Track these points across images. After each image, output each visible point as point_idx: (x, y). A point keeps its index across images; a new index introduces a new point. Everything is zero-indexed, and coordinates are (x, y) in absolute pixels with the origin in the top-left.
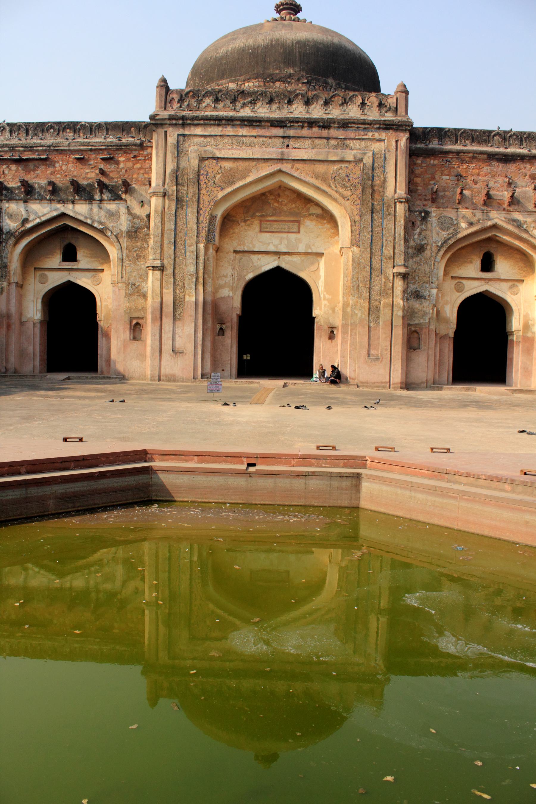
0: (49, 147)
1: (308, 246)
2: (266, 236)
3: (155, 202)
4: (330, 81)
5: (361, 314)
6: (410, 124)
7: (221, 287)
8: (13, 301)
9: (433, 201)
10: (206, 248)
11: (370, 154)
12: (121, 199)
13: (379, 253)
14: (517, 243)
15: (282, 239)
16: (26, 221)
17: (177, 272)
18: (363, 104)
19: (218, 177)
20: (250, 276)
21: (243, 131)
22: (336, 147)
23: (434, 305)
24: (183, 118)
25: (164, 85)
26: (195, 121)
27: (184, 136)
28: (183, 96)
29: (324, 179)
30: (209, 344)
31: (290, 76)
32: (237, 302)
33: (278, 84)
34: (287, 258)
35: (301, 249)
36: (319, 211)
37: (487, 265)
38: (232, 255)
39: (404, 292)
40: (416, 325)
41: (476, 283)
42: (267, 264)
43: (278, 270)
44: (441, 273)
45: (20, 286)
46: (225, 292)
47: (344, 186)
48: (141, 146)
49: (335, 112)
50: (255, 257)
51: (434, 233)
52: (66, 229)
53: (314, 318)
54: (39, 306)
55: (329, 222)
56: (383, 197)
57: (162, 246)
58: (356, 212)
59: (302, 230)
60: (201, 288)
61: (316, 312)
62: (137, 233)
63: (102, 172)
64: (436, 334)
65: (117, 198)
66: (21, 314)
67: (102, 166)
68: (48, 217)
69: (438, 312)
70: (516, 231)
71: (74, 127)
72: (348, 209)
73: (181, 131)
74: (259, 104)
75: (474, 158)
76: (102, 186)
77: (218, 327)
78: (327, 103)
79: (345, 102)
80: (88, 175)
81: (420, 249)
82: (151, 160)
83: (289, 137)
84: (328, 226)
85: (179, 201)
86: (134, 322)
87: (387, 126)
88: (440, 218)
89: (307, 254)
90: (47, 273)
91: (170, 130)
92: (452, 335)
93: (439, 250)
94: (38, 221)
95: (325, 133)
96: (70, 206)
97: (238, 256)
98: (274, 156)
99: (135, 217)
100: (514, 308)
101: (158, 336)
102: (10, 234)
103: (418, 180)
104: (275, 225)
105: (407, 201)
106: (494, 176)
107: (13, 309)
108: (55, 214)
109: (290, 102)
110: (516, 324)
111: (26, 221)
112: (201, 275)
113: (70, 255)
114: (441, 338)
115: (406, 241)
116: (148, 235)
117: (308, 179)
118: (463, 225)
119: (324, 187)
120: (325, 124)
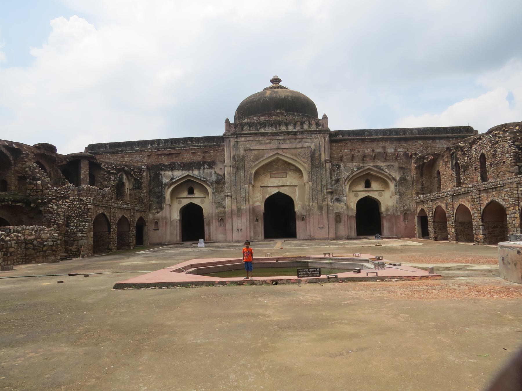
0: (181, 148)
1: (291, 182)
2: (273, 180)
3: (227, 170)
4: (296, 113)
5: (315, 210)
6: (330, 130)
7: (256, 201)
8: (168, 212)
9: (341, 160)
10: (249, 186)
11: (314, 144)
12: (212, 168)
13: (320, 184)
14: (379, 175)
15: (280, 180)
16: (172, 179)
17: (237, 197)
18: (309, 124)
19: (252, 157)
20: (267, 196)
21: (261, 138)
22: (300, 142)
23: (346, 204)
24: (237, 134)
25: (227, 121)
26: (241, 135)
27: (237, 141)
28: (235, 125)
29: (296, 156)
30: (252, 226)
31: (278, 113)
32: (262, 208)
33: (274, 117)
34: (283, 188)
35: (288, 184)
36: (294, 168)
37: (368, 185)
38: (259, 188)
39: (332, 199)
40: (338, 213)
41: (363, 193)
42: (274, 191)
43: (279, 193)
44: (347, 190)
45: (170, 206)
46: (258, 204)
47: (304, 158)
48: (219, 146)
49: (298, 128)
50: (269, 189)
51: (343, 174)
52: (189, 180)
53: (295, 213)
54: (179, 214)
55: (298, 172)
56: (320, 161)
57: (231, 187)
58: (309, 168)
59: (288, 176)
60: (247, 203)
61: (296, 210)
62: (220, 181)
63: (204, 157)
64: (348, 216)
65: (210, 167)
66: (171, 217)
67: (203, 155)
68: (182, 176)
69: (347, 207)
70: (378, 170)
71: (191, 139)
72: (306, 167)
73: (236, 140)
74: (267, 127)
75: (357, 141)
76: (205, 163)
77: (255, 218)
78: (295, 125)
79: (302, 123)
80: (198, 158)
81: (338, 181)
82: (224, 151)
83: (280, 140)
84: (298, 174)
85: (238, 168)
86: (220, 218)
87: (320, 132)
88: (345, 167)
89: (290, 186)
90: (181, 200)
91: (231, 139)
92: (355, 215)
93: (346, 180)
94: (178, 178)
95: (294, 137)
96: (191, 172)
97: (262, 189)
98: (275, 148)
99: (218, 175)
100: (381, 202)
101: (231, 224)
102: (166, 184)
103: (335, 152)
104: (277, 175)
105: (330, 162)
106: (367, 148)
107: (168, 216)
108: (185, 175)
109: (280, 125)
110: (383, 209)
111: (172, 179)
112: (247, 197)
113: (191, 192)
114: (350, 217)
115: (331, 178)
116: (225, 182)
117: (289, 156)
118: (355, 169)
119: (296, 159)
120: (295, 133)
